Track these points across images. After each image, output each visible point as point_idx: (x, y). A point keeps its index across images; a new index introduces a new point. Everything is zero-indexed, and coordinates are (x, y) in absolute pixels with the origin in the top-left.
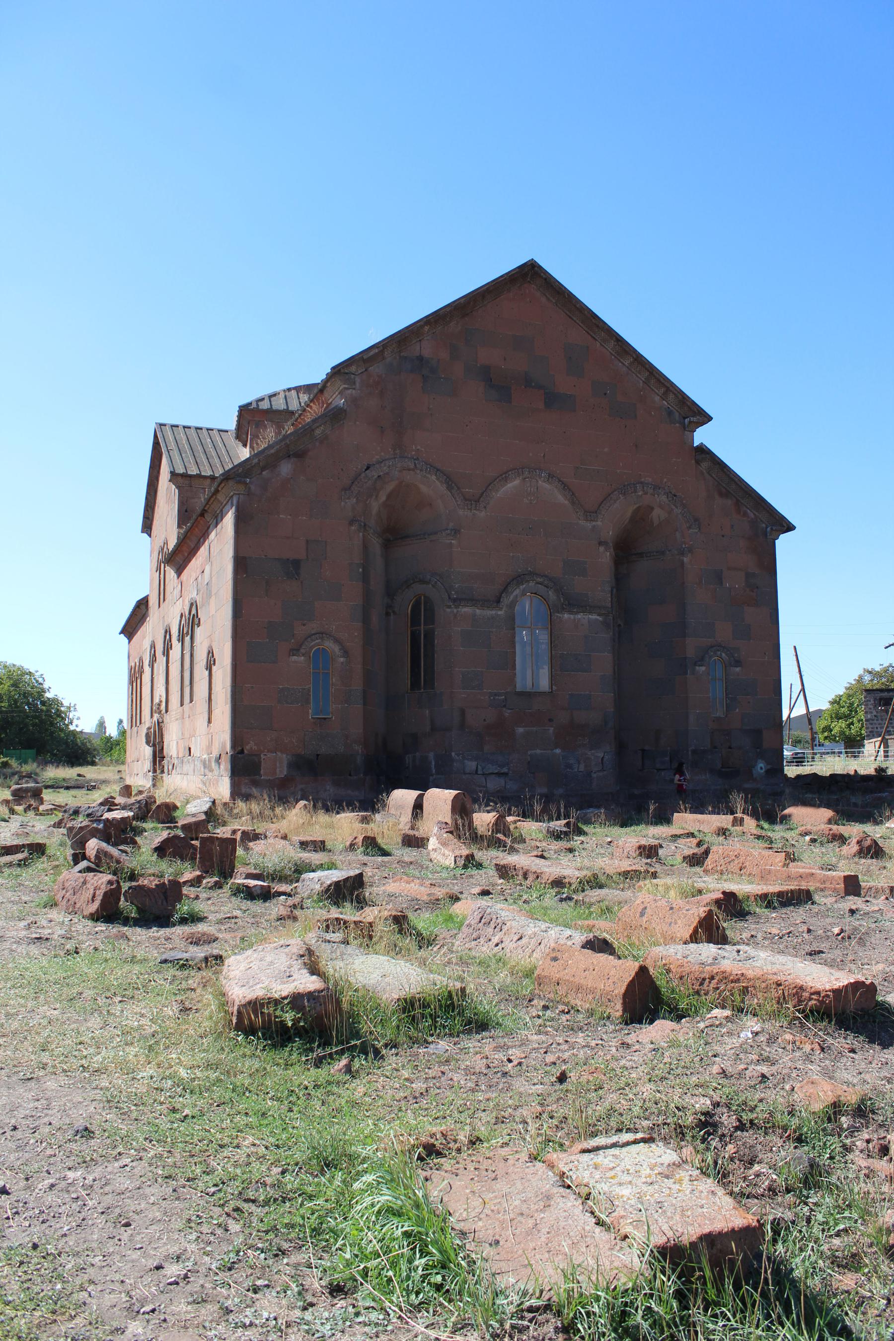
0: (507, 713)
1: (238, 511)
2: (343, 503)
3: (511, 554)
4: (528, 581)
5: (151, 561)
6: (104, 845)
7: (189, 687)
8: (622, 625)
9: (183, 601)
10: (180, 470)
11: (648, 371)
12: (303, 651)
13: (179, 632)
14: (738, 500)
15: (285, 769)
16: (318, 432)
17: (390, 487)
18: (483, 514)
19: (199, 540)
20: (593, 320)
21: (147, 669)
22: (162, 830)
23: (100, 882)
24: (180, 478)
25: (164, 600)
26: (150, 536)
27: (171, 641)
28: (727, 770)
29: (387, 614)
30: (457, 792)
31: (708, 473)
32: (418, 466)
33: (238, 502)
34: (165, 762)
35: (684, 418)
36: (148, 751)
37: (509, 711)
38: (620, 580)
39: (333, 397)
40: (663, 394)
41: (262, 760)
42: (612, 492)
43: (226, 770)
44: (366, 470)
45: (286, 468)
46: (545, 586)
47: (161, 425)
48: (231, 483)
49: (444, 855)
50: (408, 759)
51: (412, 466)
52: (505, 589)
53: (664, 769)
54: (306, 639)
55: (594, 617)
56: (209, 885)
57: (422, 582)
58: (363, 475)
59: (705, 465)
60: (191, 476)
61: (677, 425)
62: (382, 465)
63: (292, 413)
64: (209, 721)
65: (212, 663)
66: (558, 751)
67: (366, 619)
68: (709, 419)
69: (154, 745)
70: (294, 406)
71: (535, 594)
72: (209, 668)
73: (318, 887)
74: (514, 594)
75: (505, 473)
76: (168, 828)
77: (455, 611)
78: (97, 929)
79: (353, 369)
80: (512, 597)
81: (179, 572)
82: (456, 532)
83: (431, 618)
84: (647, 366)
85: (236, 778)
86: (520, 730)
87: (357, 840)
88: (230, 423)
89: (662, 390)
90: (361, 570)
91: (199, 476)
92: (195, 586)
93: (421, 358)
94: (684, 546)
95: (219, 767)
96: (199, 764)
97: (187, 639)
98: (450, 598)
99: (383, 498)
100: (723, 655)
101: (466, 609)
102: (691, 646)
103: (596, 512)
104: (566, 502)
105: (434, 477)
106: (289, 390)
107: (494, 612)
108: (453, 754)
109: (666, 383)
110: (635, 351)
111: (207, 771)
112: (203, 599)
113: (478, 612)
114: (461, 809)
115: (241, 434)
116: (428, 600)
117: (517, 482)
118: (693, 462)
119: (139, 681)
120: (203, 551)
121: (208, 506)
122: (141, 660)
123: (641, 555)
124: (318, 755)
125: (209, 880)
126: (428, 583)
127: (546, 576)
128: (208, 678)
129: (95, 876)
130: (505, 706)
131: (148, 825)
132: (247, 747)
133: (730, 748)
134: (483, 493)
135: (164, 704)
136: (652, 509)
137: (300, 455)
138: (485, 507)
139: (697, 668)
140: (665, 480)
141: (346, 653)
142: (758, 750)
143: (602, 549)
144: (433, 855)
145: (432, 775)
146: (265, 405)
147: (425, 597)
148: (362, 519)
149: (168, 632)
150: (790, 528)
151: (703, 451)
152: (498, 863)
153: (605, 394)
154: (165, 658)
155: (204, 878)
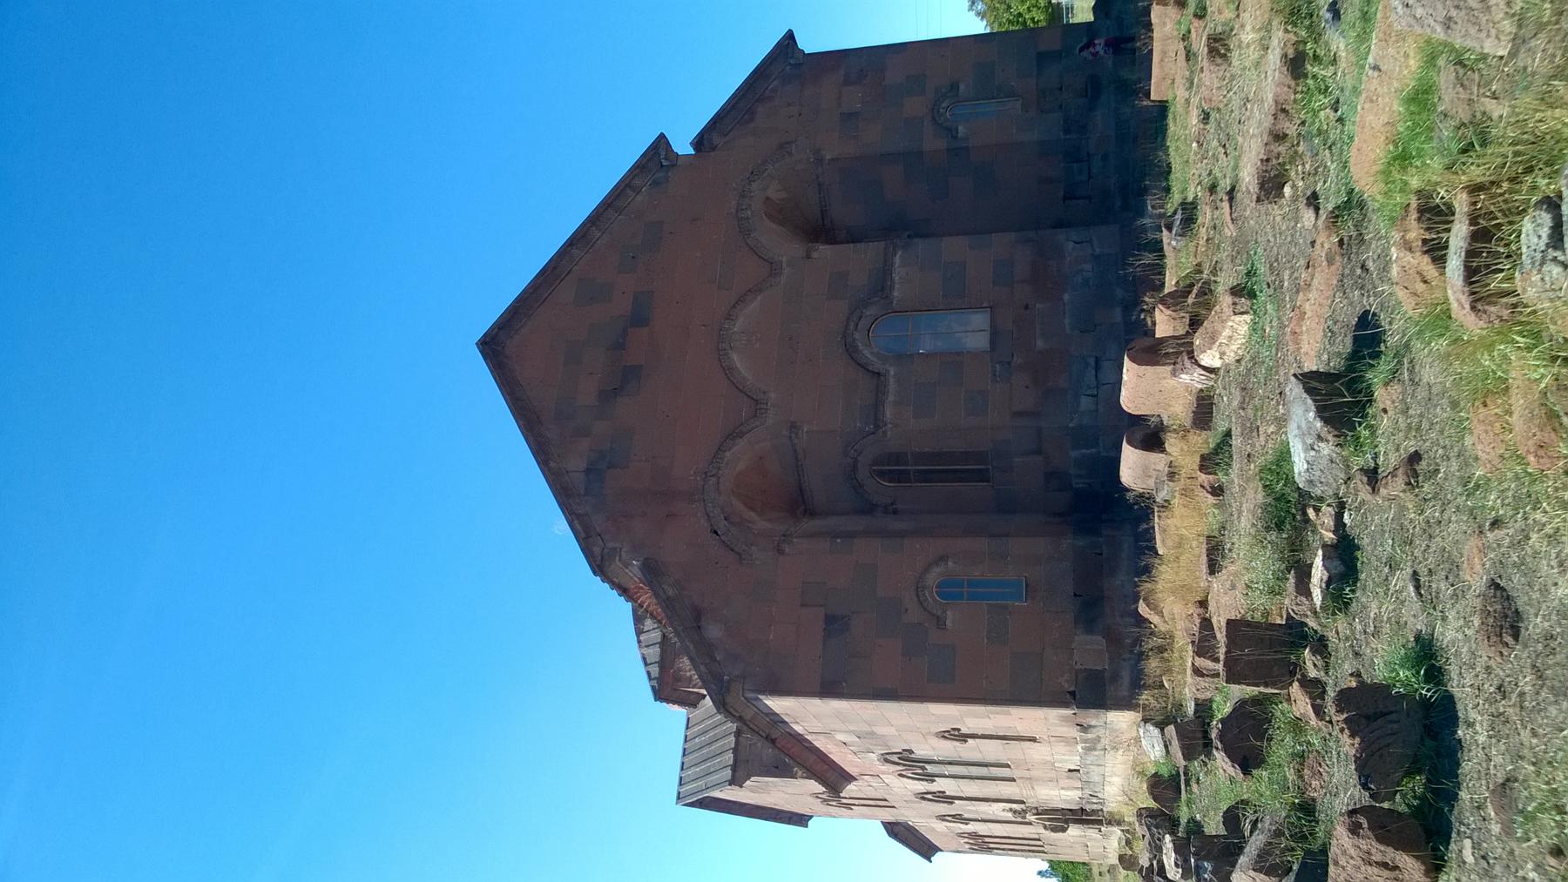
0: (1017, 360)
1: (763, 692)
2: (757, 563)
4: (854, 340)
5: (841, 816)
6: (1243, 860)
7: (991, 768)
8: (907, 234)
9: (884, 773)
10: (728, 773)
11: (607, 209)
12: (939, 613)
13: (922, 780)
14: (757, 101)
15: (1094, 638)
16: (671, 592)
17: (739, 506)
18: (773, 395)
19: (807, 748)
21: (971, 827)
22: (1191, 793)
23: (1352, 852)
24: (737, 774)
25: (885, 800)
26: (811, 817)
27: (934, 793)
28: (1089, 90)
29: (895, 512)
30: (1126, 357)
31: (726, 135)
32: (713, 473)
33: (753, 691)
34: (1088, 807)
35: (662, 166)
36: (1074, 831)
37: (1015, 359)
38: (854, 237)
39: (632, 575)
40: (634, 191)
41: (1083, 667)
42: (747, 244)
43: (1097, 717)
44: (718, 535)
45: (713, 631)
47: (678, 798)
48: (729, 699)
49: (1230, 337)
50: (1079, 484)
51: (714, 479)
52: (862, 367)
53: (1089, 168)
54: (925, 609)
55: (897, 260)
56: (1320, 663)
57: (854, 468)
58: (723, 538)
60: (735, 761)
62: (712, 515)
63: (664, 636)
64: (1033, 740)
65: (957, 733)
66: (1066, 297)
67: (901, 534)
68: (662, 136)
69: (1067, 821)
70: (656, 636)
72: (964, 738)
73: (1326, 449)
75: (724, 369)
76: (1187, 784)
77: (890, 426)
78: (1469, 859)
79: (597, 550)
81: (850, 778)
82: (793, 427)
83: (898, 458)
84: (602, 210)
85: (1108, 702)
86: (1040, 344)
87: (1205, 485)
88: (678, 713)
89: (629, 191)
90: (839, 540)
91: (735, 750)
92: (863, 755)
93: (588, 471)
94: (812, 160)
95: (1094, 727)
96: (1090, 759)
97: (930, 768)
98: (873, 433)
100: (944, 105)
101: (889, 413)
102: (933, 143)
103: (772, 263)
104: (759, 298)
105: (728, 454)
106: (639, 642)
107: (892, 380)
108: (1071, 425)
110: (583, 225)
111: (1099, 746)
112: (875, 745)
113: (891, 398)
114: (1153, 353)
115: (690, 702)
116: (875, 463)
117: (735, 357)
118: (712, 154)
119: (987, 840)
120: (820, 743)
121: (761, 732)
122: (960, 835)
123: (824, 213)
124: (1075, 595)
125: (1309, 664)
126: (856, 461)
127: (848, 319)
128: (977, 740)
129: (1336, 863)
130: (1009, 363)
131: (1184, 814)
132: (1066, 686)
133: (1061, 89)
134: (749, 397)
135: (1015, 806)
136: (767, 198)
137: (698, 614)
139: (959, 135)
140: (734, 185)
141: (943, 559)
142: (1063, 54)
143: (815, 255)
144: (1231, 357)
145: (1099, 453)
146: (655, 670)
147: (874, 465)
148: (778, 538)
149: (922, 796)
150: (790, 36)
151: (699, 143)
152: (1255, 197)
153: (633, 257)
154: (957, 802)
155: (1304, 676)
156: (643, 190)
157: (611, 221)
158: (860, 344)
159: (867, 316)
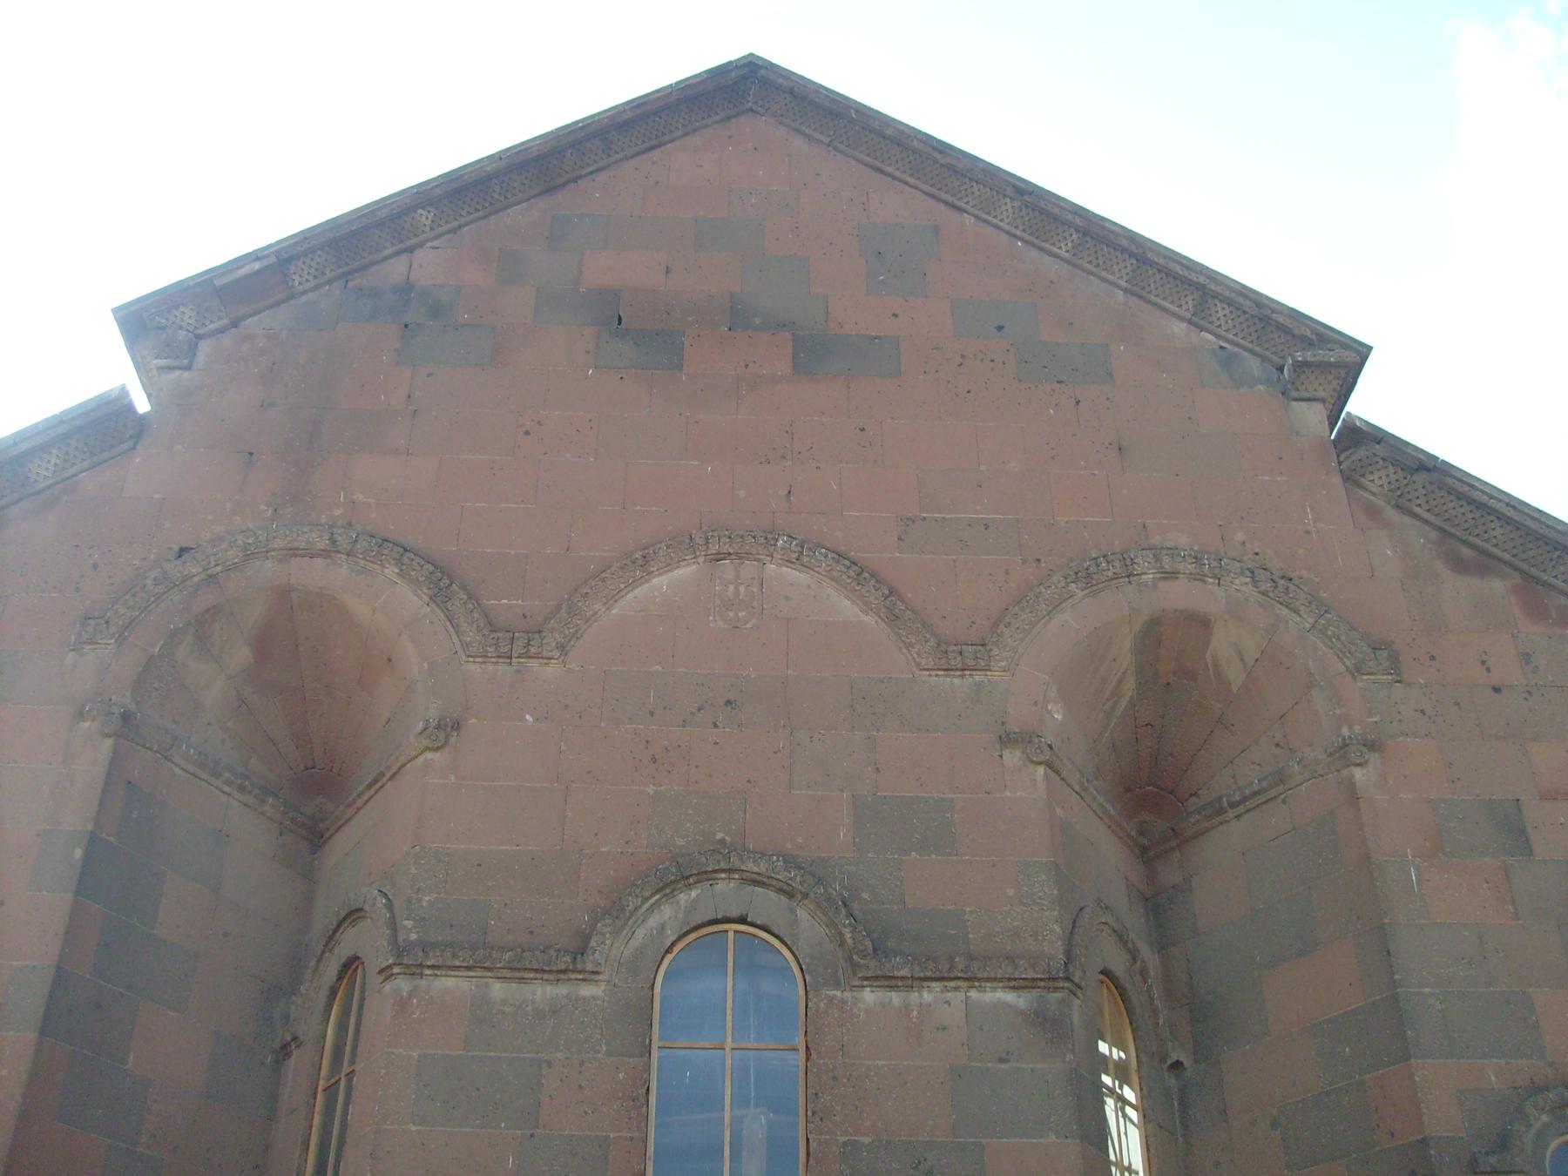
3: (651, 789)
11: (1131, 255)
18: (552, 670)
20: (939, 157)
40: (1194, 314)
46: (780, 891)
59: (1378, 481)
61: (1261, 387)
71: (742, 920)
74: (654, 921)
80: (641, 933)
89: (1189, 303)
99: (243, 656)
101: (448, 982)
104: (870, 619)
105: (391, 571)
107: (563, 990)
109: (1193, 277)
117: (684, 572)
118: (1336, 480)
138: (561, 647)
140: (1240, 536)
143: (1012, 757)
156: (1204, 334)
157: (1104, 274)
158: (694, 894)
159: (793, 911)
